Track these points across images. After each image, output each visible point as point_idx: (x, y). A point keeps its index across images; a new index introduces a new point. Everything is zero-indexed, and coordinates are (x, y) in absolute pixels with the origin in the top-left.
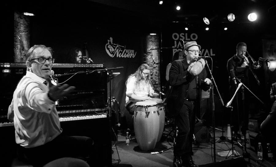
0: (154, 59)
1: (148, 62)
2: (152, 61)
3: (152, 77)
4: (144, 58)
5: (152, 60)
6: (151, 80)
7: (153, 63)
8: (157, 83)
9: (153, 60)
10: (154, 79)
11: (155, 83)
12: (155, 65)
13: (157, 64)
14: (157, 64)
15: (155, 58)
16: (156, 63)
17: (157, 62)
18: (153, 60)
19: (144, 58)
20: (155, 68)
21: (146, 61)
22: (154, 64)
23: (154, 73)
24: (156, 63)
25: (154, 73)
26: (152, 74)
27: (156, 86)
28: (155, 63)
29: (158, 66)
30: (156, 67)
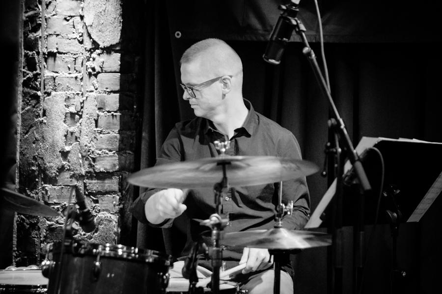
0: (88, 20)
1: (53, 39)
2: (82, 31)
3: (71, 129)
4: (31, 13)
5: (80, 27)
6: (67, 148)
7: (88, 44)
8: (100, 167)
9: (86, 27)
10: (85, 140)
11: (91, 166)
12: (99, 60)
13: (109, 50)
14: (109, 50)
15: (98, 15)
16: (102, 46)
17: (111, 35)
18: (86, 27)
19: (31, 13)
20: (93, 74)
21: (39, 33)
22: (91, 51)
23: (90, 108)
24: (102, 46)
25: (90, 108)
26: (72, 109)
27: (94, 185)
28: (96, 46)
29: (114, 61)
30: (102, 71)
